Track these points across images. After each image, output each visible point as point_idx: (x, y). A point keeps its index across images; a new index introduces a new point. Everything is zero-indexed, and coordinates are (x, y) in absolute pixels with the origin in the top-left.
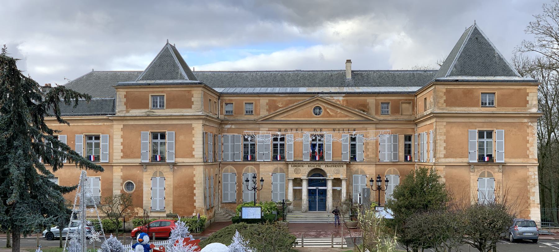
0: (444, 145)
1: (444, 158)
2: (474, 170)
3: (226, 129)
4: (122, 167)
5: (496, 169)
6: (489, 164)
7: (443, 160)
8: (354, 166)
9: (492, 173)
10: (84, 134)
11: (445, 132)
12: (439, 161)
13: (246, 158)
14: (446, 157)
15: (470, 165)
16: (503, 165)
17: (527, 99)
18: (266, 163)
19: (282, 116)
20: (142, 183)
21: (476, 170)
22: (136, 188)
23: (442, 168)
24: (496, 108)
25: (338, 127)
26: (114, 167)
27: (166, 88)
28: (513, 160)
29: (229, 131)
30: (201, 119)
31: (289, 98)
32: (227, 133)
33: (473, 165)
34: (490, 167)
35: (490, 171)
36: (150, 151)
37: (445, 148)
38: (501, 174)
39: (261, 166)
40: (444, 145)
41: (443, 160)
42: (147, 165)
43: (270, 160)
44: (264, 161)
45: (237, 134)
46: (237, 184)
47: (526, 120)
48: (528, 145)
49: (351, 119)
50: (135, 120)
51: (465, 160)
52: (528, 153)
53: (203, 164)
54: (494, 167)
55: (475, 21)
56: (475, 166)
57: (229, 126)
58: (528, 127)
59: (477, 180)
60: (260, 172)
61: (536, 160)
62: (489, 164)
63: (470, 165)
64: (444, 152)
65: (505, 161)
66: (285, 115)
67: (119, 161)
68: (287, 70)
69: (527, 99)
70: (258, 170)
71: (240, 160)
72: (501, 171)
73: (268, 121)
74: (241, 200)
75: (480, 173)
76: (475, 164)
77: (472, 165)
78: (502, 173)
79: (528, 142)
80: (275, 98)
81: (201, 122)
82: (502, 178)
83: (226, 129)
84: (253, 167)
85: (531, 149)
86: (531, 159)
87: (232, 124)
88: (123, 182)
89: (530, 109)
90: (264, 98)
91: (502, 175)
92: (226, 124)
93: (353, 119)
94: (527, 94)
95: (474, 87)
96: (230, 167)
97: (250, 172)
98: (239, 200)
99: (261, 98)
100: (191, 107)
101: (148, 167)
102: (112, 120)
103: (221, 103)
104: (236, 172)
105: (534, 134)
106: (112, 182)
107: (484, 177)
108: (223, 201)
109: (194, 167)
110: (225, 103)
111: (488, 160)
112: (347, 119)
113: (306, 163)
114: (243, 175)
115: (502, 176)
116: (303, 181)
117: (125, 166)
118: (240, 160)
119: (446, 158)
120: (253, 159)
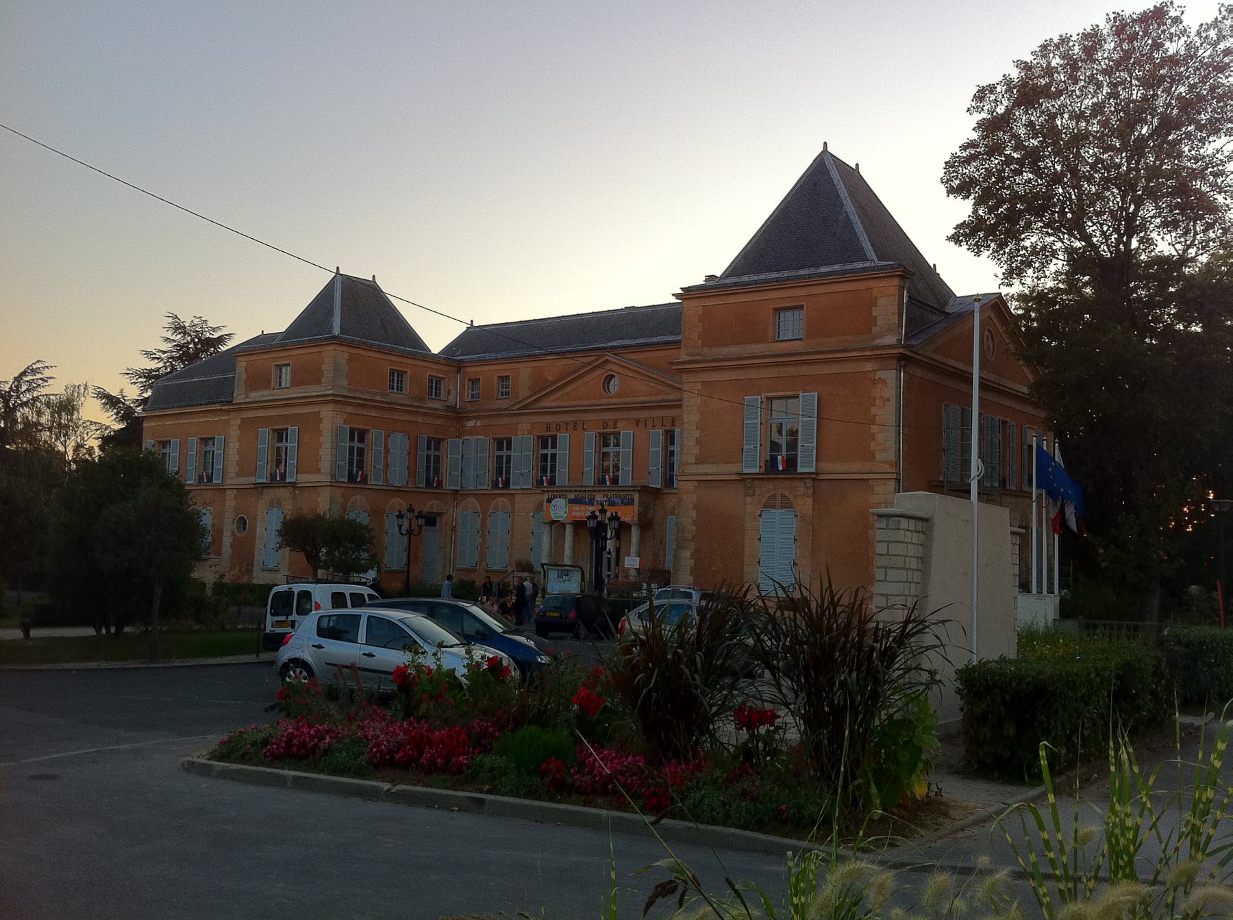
0: (697, 434)
1: (695, 464)
2: (754, 491)
3: (469, 428)
4: (235, 492)
5: (800, 488)
6: (782, 476)
7: (693, 469)
8: (671, 496)
9: (791, 497)
10: (199, 436)
11: (699, 404)
12: (686, 471)
13: (495, 485)
14: (700, 460)
15: (744, 480)
16: (814, 479)
17: (874, 314)
18: (524, 492)
19: (552, 398)
20: (257, 520)
21: (758, 491)
22: (249, 524)
23: (691, 486)
24: (803, 342)
25: (643, 415)
26: (228, 491)
27: (282, 352)
28: (838, 467)
29: (473, 431)
30: (330, 402)
31: (564, 362)
32: (469, 435)
33: (750, 479)
34: (787, 483)
35: (786, 493)
36: (269, 463)
37: (698, 442)
38: (810, 501)
39: (518, 498)
40: (697, 434)
41: (693, 469)
42: (263, 486)
43: (530, 487)
44: (522, 489)
45: (483, 437)
46: (480, 533)
47: (869, 366)
48: (874, 429)
49: (667, 397)
50: (252, 409)
51: (734, 468)
52: (872, 449)
53: (329, 484)
54: (796, 483)
55: (825, 143)
56: (756, 482)
57: (471, 423)
58: (875, 382)
59: (757, 515)
60: (516, 511)
61: (890, 464)
62: (782, 476)
63: (743, 479)
64: (696, 450)
65: (816, 468)
66: (558, 394)
67: (234, 482)
68: (595, 311)
69: (874, 314)
70: (513, 505)
71: (486, 487)
72: (810, 491)
73: (531, 407)
74: (484, 564)
75: (765, 499)
76: (754, 478)
77: (748, 478)
78: (811, 499)
79: (873, 420)
80: (541, 364)
81: (331, 406)
82: (813, 510)
83: (469, 428)
84: (506, 500)
85: (880, 437)
86: (881, 462)
87: (476, 418)
88: (236, 516)
89: (875, 338)
90: (526, 364)
91: (814, 502)
92: (468, 419)
93: (671, 397)
94: (874, 302)
95: (757, 297)
96: (471, 500)
97: (500, 510)
98: (480, 564)
99: (521, 365)
100: (319, 382)
101: (265, 491)
102: (229, 411)
103: (462, 380)
104: (480, 510)
105: (889, 400)
106: (223, 518)
107: (774, 507)
108: (458, 566)
109: (319, 489)
110: (469, 380)
111: (785, 467)
112: (660, 397)
113: (568, 489)
114: (490, 516)
115: (813, 507)
116: (567, 526)
117: (240, 490)
118: (486, 487)
119: (699, 463)
120: (507, 483)
